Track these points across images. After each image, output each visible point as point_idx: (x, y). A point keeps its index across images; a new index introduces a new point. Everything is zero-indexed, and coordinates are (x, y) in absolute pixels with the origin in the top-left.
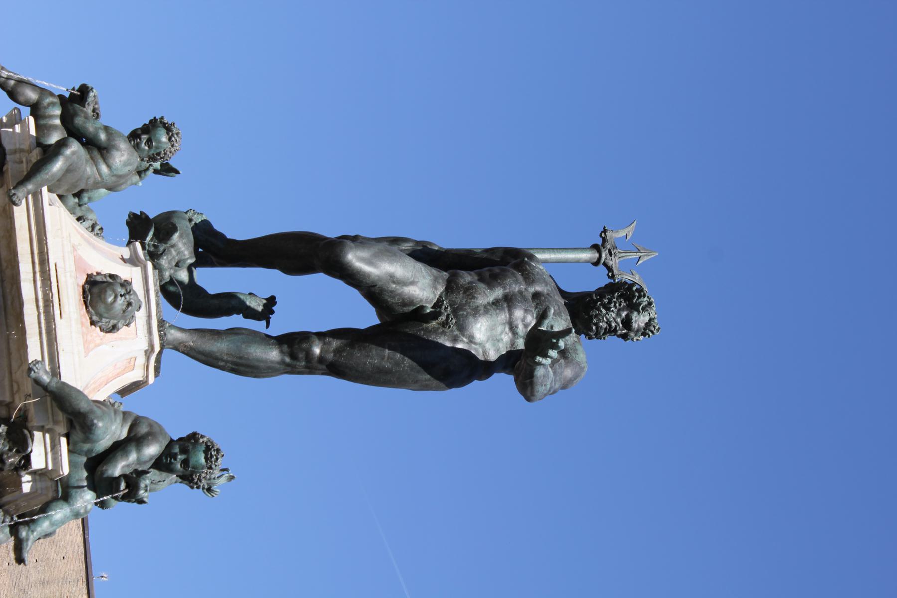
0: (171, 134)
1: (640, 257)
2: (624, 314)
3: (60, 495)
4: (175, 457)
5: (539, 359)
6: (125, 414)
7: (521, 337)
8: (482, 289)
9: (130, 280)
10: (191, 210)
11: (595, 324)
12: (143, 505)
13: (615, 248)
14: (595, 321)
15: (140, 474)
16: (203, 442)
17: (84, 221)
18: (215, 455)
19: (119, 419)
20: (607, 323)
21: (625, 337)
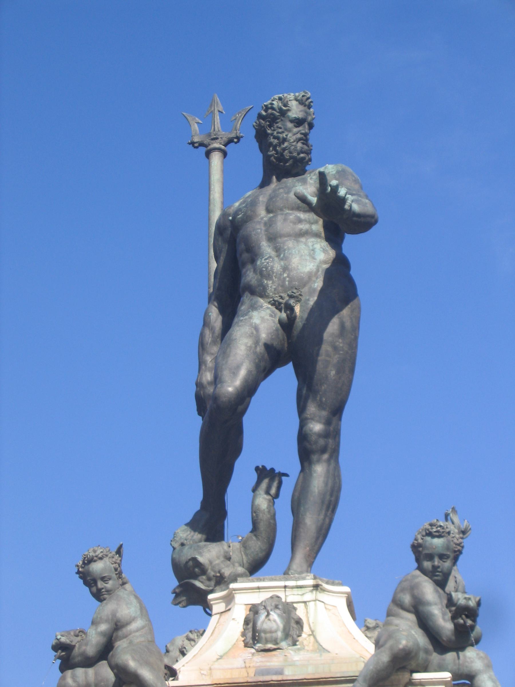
0: (95, 558)
1: (219, 111)
2: (290, 125)
3: (467, 682)
4: (435, 568)
5: (346, 207)
6: (389, 614)
7: (311, 227)
8: (263, 261)
9: (250, 606)
10: (171, 544)
11: (299, 154)
12: (482, 602)
13: (209, 135)
14: (295, 154)
15: (450, 602)
16: (422, 539)
17: (185, 648)
18: (437, 528)
19: (396, 621)
20: (297, 142)
21: (311, 126)
